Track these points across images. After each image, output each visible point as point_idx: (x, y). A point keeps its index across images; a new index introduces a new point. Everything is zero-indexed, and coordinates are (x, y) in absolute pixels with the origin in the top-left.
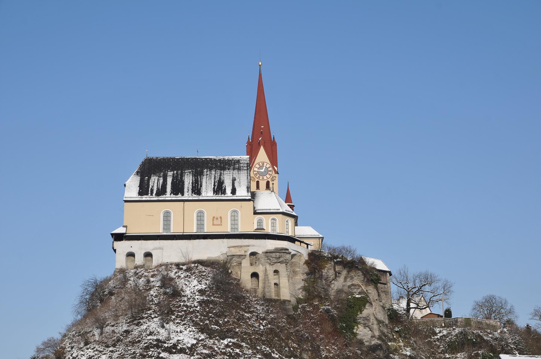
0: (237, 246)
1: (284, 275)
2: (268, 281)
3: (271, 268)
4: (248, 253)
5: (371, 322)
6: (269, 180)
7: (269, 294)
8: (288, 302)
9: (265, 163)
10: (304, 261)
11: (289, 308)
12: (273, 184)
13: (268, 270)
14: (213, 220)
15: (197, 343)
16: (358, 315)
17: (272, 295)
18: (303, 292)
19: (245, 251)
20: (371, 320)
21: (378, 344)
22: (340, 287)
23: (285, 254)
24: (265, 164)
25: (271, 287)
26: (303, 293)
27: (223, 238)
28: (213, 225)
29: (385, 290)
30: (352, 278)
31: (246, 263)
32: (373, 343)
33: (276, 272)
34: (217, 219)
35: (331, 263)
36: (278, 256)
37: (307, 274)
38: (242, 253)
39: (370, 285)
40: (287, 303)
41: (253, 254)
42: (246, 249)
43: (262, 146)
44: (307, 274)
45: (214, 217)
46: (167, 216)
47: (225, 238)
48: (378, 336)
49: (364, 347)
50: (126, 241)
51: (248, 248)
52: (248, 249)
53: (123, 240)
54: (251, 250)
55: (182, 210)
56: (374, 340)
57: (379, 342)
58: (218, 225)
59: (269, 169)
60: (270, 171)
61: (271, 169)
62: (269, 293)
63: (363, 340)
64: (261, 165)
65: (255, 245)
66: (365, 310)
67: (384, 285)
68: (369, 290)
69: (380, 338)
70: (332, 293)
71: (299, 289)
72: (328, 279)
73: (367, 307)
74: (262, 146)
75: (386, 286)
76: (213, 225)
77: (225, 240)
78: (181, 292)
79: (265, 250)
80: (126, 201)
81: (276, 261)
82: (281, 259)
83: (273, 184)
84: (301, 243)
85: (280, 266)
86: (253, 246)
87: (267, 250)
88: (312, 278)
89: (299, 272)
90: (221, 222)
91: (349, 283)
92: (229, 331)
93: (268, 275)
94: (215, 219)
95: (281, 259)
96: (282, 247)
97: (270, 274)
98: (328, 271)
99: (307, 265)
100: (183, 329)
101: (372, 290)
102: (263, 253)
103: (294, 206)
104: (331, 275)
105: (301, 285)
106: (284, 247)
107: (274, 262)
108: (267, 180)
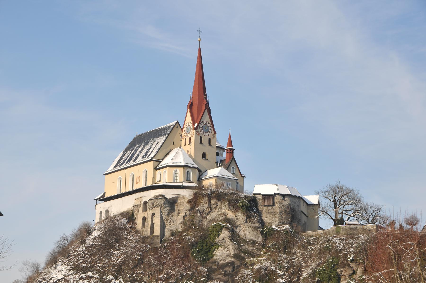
3: (150, 212)
4: (142, 203)
5: (227, 243)
6: (191, 136)
7: (146, 232)
8: (157, 237)
10: (187, 200)
11: (157, 242)
15: (62, 278)
16: (216, 239)
17: (148, 233)
18: (182, 226)
19: (141, 202)
20: (227, 242)
21: (230, 262)
22: (214, 217)
23: (157, 200)
24: (190, 123)
25: (148, 227)
26: (182, 227)
27: (133, 193)
29: (273, 211)
30: (221, 208)
31: (141, 209)
32: (227, 261)
35: (205, 199)
36: (152, 203)
37: (189, 210)
38: (138, 203)
39: (238, 212)
40: (156, 238)
41: (145, 203)
42: (140, 200)
44: (189, 210)
45: (137, 177)
47: (142, 191)
48: (233, 254)
49: (214, 266)
51: (142, 198)
52: (142, 200)
55: (125, 175)
56: (228, 259)
57: (233, 260)
61: (192, 127)
62: (146, 232)
63: (217, 259)
64: (188, 125)
65: (145, 196)
66: (222, 234)
67: (271, 207)
68: (238, 215)
69: (235, 256)
70: (205, 222)
71: (180, 224)
72: (204, 212)
73: (223, 232)
75: (273, 207)
78: (89, 241)
80: (106, 174)
81: (152, 206)
82: (155, 204)
84: (101, 201)
85: (156, 209)
86: (145, 196)
87: (151, 198)
88: (192, 213)
89: (183, 210)
91: (219, 213)
92: (92, 267)
93: (148, 218)
95: (155, 204)
96: (159, 194)
97: (149, 217)
98: (203, 205)
99: (189, 203)
100: (63, 269)
101: (240, 215)
103: (234, 150)
104: (206, 208)
105: (181, 221)
106: (160, 194)
107: (151, 207)
108: (189, 137)
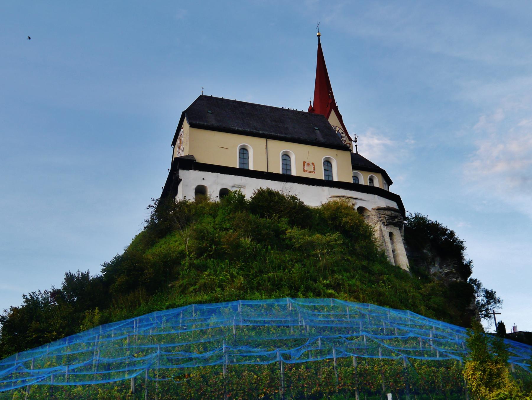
0: (343, 197)
1: (400, 241)
2: (385, 243)
4: (356, 208)
9: (337, 128)
12: (356, 146)
13: (382, 230)
14: (304, 165)
28: (304, 171)
33: (391, 234)
34: (308, 164)
42: (354, 201)
43: (333, 110)
45: (304, 162)
46: (244, 151)
50: (196, 171)
52: (356, 203)
53: (191, 170)
54: (359, 204)
58: (310, 172)
59: (342, 135)
60: (344, 137)
74: (333, 110)
76: (304, 171)
77: (326, 189)
79: (375, 206)
83: (356, 146)
90: (314, 169)
91: (446, 271)
94: (306, 164)
95: (396, 220)
102: (373, 209)
